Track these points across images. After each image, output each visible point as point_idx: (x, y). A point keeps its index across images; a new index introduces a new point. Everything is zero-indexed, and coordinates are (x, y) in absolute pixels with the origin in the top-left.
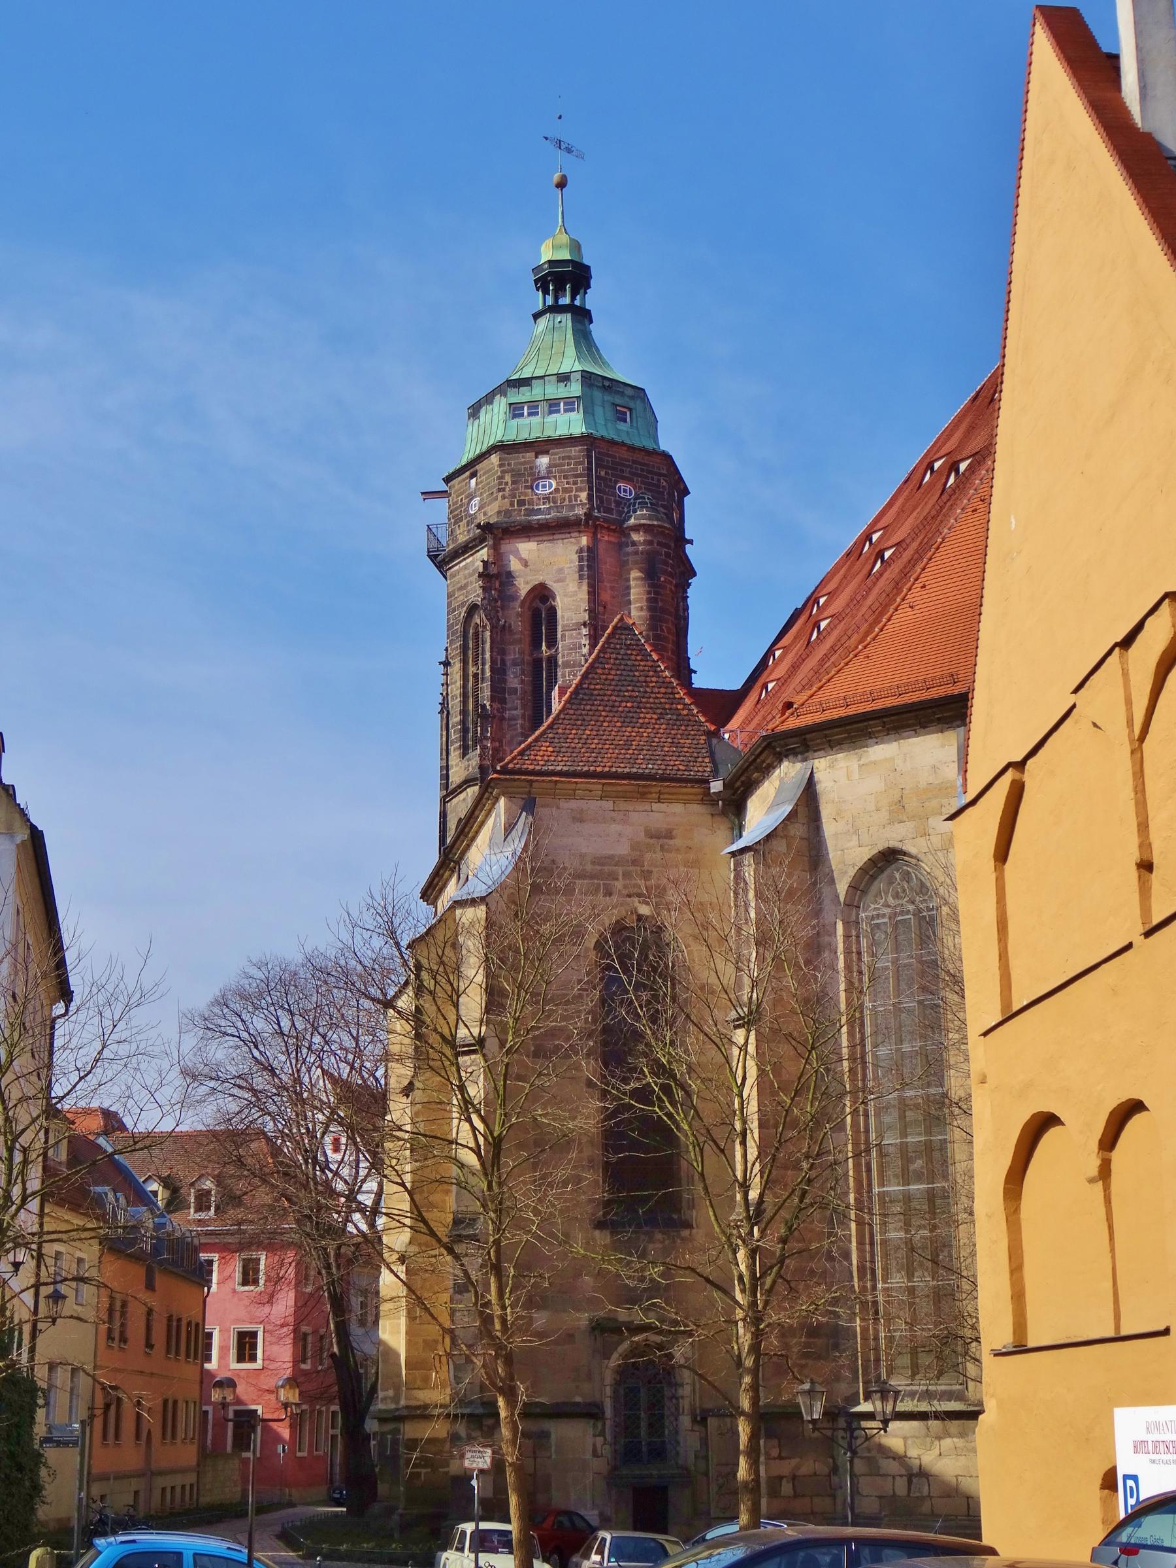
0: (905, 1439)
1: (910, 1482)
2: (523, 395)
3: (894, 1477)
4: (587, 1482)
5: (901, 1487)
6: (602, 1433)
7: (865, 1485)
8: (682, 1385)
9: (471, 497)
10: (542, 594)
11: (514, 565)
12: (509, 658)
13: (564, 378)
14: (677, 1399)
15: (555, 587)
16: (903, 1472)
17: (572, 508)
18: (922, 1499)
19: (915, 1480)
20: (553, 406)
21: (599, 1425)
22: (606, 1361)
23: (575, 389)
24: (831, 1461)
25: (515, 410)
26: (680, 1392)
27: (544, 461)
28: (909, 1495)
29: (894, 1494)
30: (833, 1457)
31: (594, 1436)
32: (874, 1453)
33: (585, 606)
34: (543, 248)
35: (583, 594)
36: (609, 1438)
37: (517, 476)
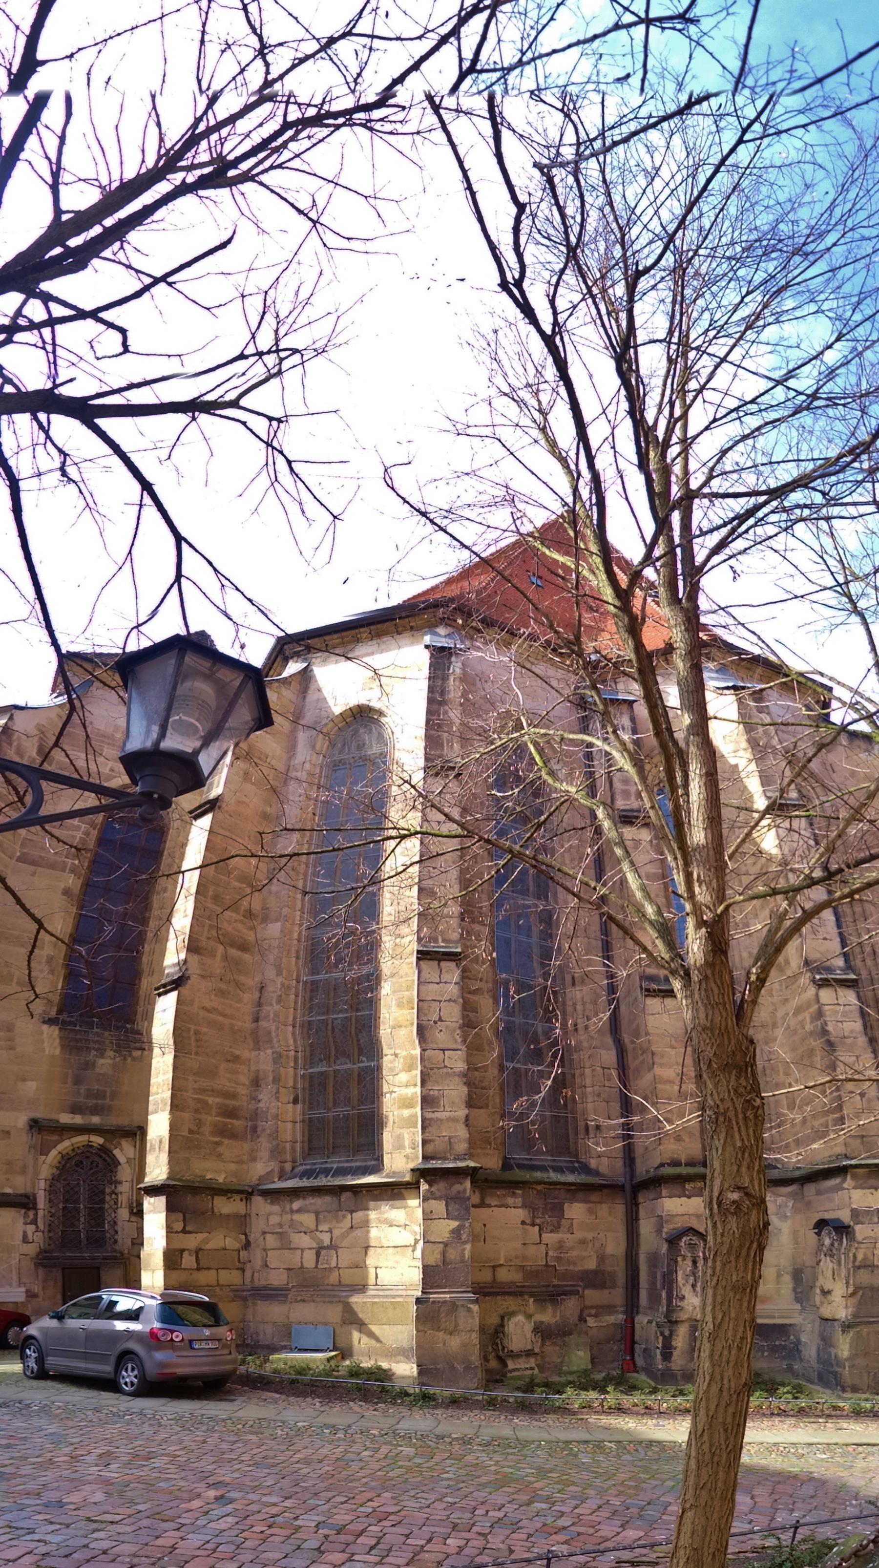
0: (317, 1214)
1: (318, 1255)
3: (302, 1250)
4: (13, 1262)
5: (309, 1259)
6: (34, 1222)
7: (274, 1259)
8: (121, 1183)
14: (116, 1194)
16: (314, 1245)
18: (331, 1269)
19: (323, 1252)
21: (31, 1214)
22: (43, 1157)
24: (243, 1237)
26: (120, 1188)
28: (316, 1267)
29: (302, 1267)
30: (246, 1234)
31: (26, 1224)
32: (286, 1228)
36: (41, 1226)
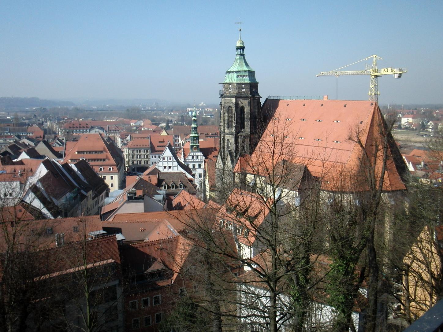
2: (239, 74)
9: (230, 88)
10: (243, 108)
11: (240, 102)
12: (238, 117)
13: (245, 71)
15: (245, 106)
17: (247, 94)
20: (244, 76)
23: (247, 74)
25: (238, 76)
27: (243, 86)
33: (249, 110)
34: (237, 42)
35: (249, 108)
37: (239, 88)
